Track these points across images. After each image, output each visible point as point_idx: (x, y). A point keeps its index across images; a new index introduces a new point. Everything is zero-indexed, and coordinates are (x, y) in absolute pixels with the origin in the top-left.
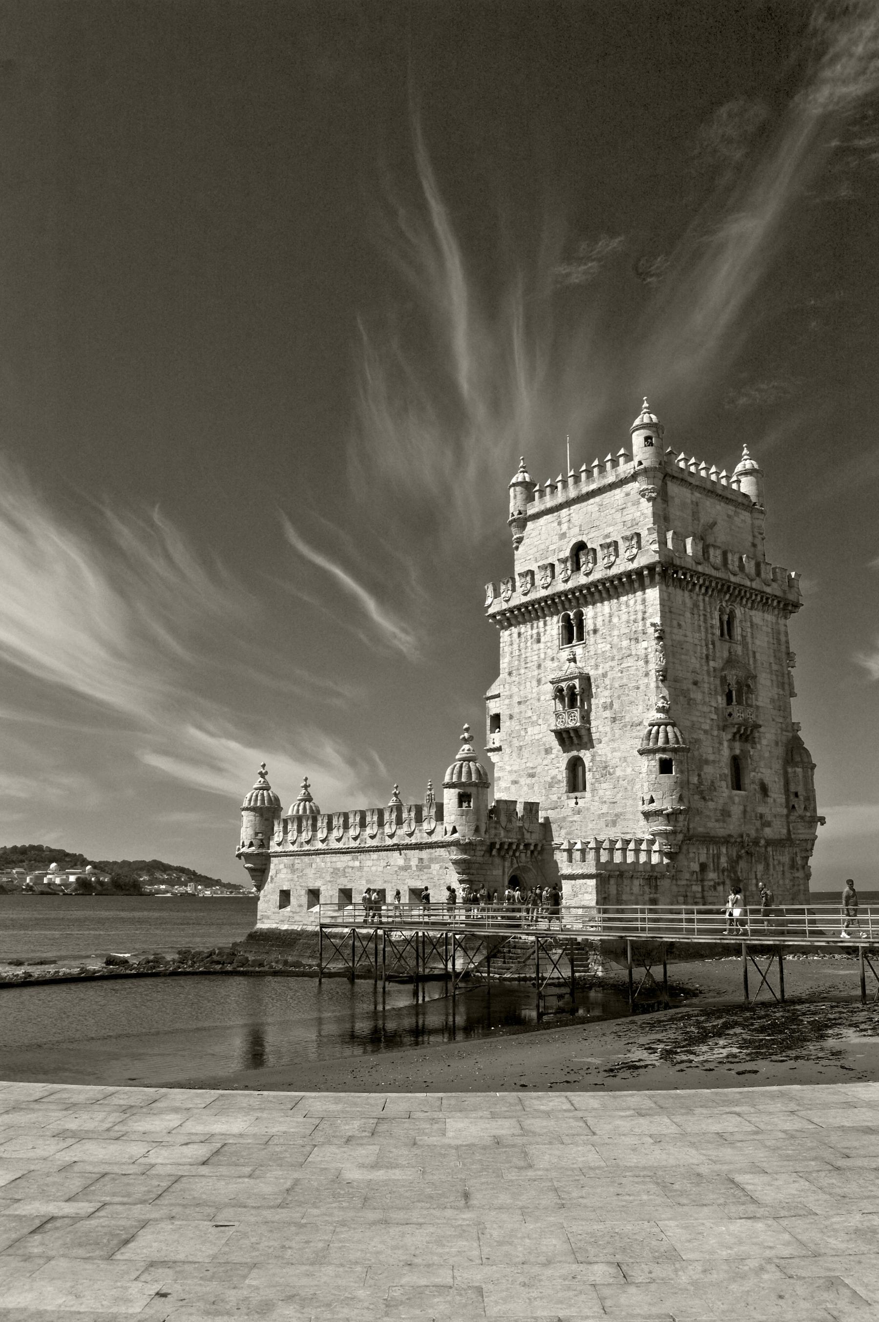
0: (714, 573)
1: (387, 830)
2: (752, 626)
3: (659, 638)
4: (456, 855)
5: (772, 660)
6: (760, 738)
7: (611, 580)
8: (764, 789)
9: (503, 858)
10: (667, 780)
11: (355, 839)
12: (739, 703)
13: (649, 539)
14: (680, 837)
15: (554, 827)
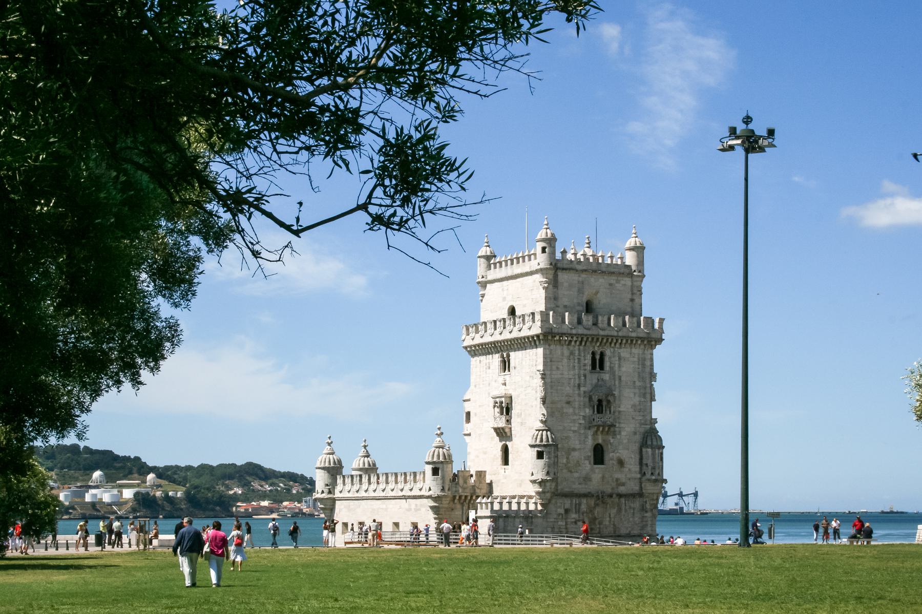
0: (586, 332)
1: (400, 486)
2: (620, 359)
3: (542, 378)
4: (432, 503)
5: (636, 379)
6: (620, 432)
7: (521, 338)
8: (621, 463)
9: (462, 504)
10: (541, 462)
11: (383, 490)
12: (600, 410)
13: (538, 317)
14: (548, 495)
15: (494, 485)
